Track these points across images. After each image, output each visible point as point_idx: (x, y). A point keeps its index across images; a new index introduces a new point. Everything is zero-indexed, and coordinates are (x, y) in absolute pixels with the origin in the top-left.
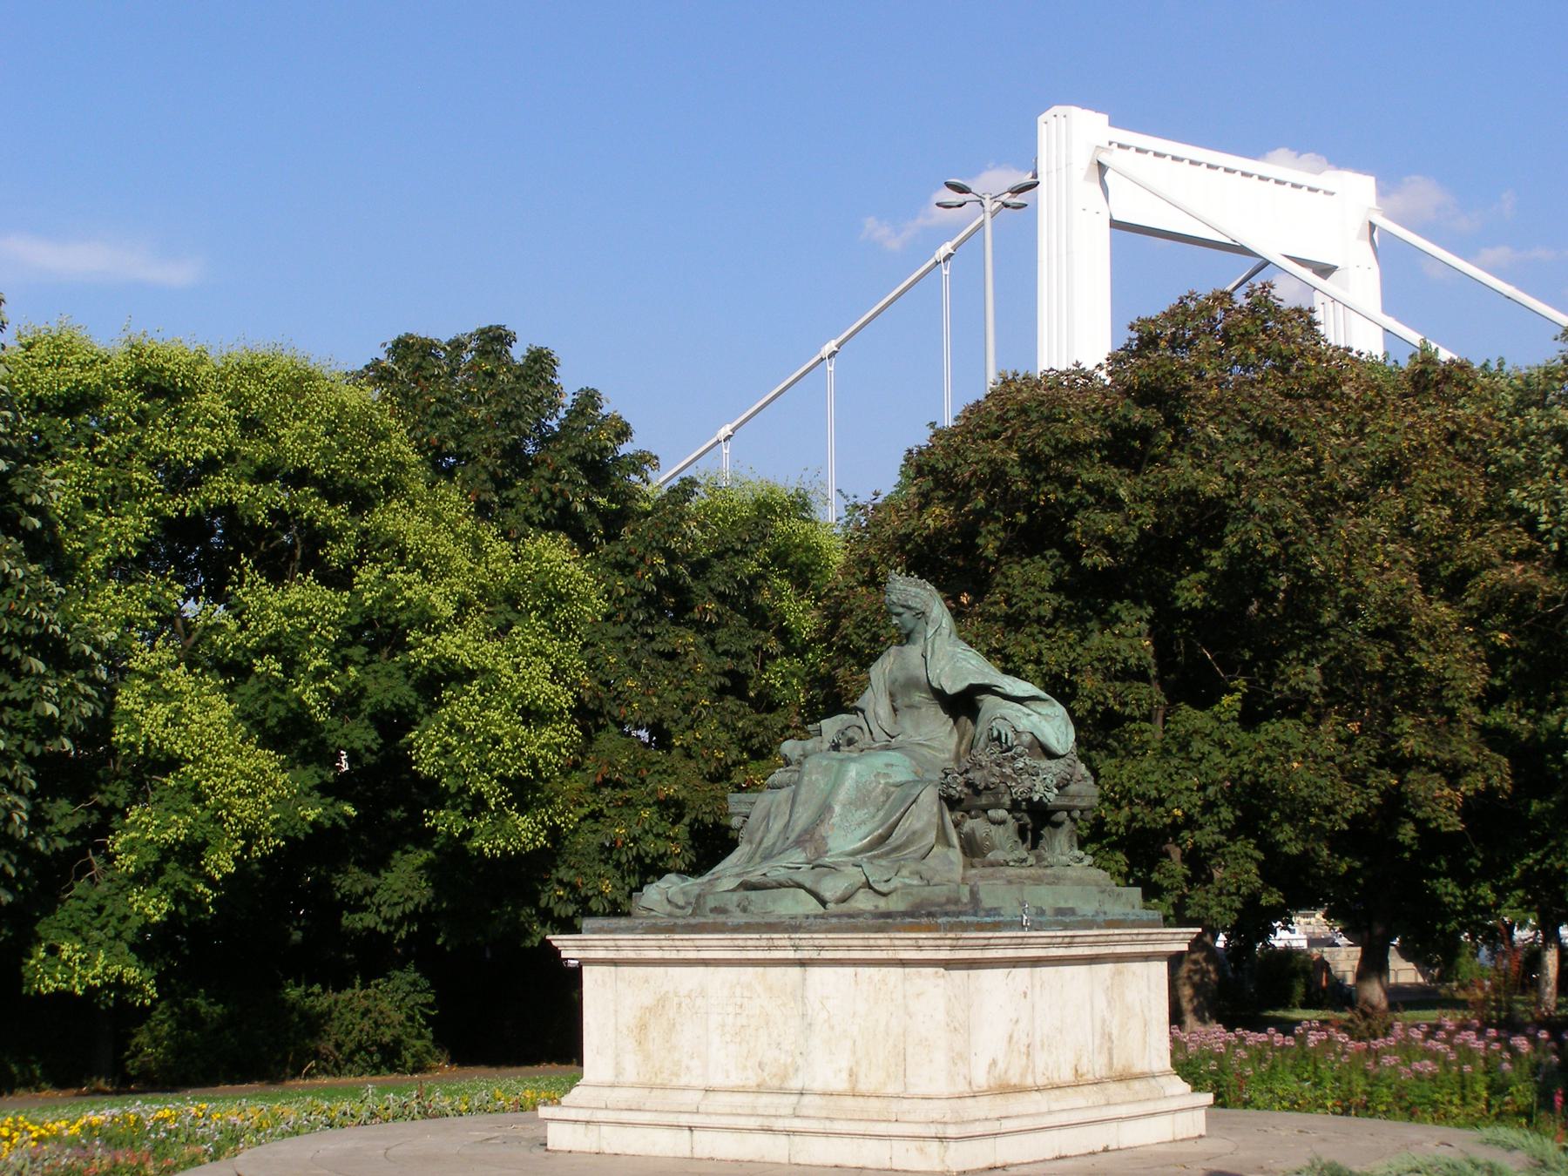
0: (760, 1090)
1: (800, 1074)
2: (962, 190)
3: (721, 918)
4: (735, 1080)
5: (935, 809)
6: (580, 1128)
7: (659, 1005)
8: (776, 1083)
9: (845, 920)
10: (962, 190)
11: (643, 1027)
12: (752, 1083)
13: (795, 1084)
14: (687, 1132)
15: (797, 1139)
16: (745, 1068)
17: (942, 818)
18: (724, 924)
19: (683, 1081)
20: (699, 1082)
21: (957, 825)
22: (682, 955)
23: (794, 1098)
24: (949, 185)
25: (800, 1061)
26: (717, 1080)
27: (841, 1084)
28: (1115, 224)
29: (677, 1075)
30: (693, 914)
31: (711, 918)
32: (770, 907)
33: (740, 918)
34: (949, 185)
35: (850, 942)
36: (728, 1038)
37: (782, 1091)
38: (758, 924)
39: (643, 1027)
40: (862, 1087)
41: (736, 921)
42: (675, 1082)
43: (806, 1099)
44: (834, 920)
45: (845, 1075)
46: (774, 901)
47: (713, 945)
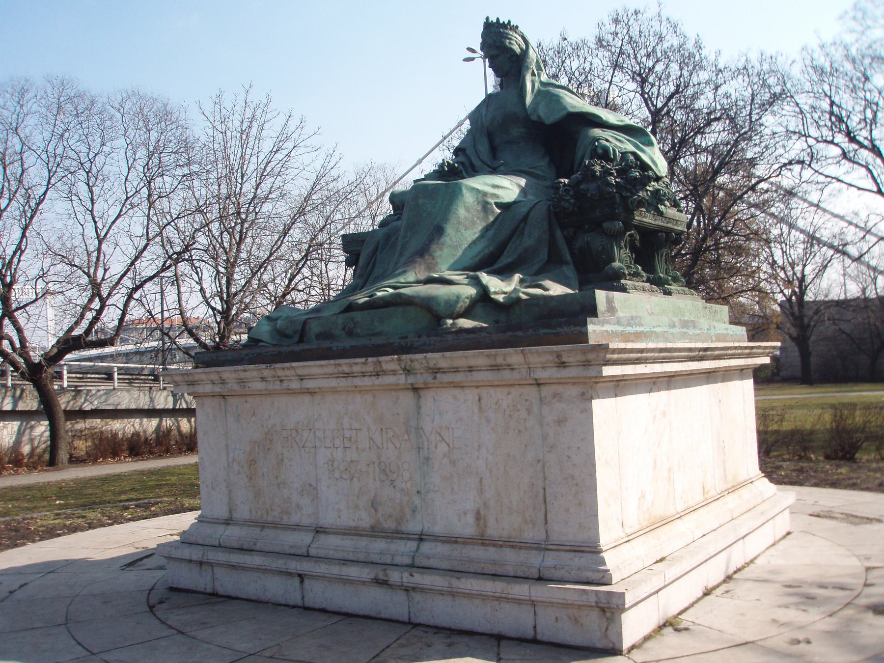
0: (375, 532)
1: (418, 517)
3: (326, 344)
4: (347, 520)
5: (546, 226)
11: (252, 462)
13: (414, 527)
14: (297, 580)
15: (417, 597)
17: (552, 235)
18: (329, 349)
21: (569, 241)
23: (412, 545)
24: (469, 49)
25: (417, 501)
26: (328, 519)
27: (467, 527)
30: (301, 341)
31: (314, 345)
33: (348, 343)
34: (469, 49)
36: (337, 475)
37: (398, 534)
39: (252, 462)
40: (493, 531)
41: (341, 345)
42: (286, 520)
45: (470, 519)
47: (317, 370)
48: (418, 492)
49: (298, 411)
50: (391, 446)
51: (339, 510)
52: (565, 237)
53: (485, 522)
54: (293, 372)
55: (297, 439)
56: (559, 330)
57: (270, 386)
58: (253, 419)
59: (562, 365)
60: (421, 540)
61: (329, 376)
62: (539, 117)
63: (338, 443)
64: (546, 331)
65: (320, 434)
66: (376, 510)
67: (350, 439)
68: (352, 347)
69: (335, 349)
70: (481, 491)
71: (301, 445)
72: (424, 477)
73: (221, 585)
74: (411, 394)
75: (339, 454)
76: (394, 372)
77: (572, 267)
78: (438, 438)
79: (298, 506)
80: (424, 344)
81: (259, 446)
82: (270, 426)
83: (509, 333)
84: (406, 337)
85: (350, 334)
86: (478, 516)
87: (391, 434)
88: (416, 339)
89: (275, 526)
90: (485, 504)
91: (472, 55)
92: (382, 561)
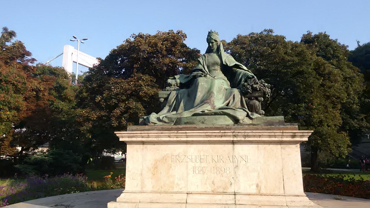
0: (214, 193)
1: (233, 186)
2: (75, 38)
7: (164, 159)
8: (221, 190)
9: (251, 126)
10: (75, 38)
11: (156, 167)
12: (209, 190)
13: (231, 190)
18: (196, 127)
19: (176, 190)
20: (185, 190)
22: (179, 139)
26: (191, 189)
27: (253, 190)
28: (74, 62)
32: (215, 122)
33: (203, 126)
35: (260, 134)
37: (224, 193)
38: (211, 127)
40: (263, 191)
42: (171, 190)
43: (238, 197)
44: (246, 126)
45: (254, 187)
46: (216, 119)
48: (233, 178)
51: (197, 185)
52: (245, 101)
53: (260, 188)
54: (185, 134)
55: (179, 159)
56: (287, 126)
57: (172, 139)
59: (294, 136)
60: (235, 194)
62: (227, 64)
63: (198, 160)
64: (282, 126)
66: (214, 185)
68: (205, 127)
70: (258, 177)
71: (181, 161)
72: (235, 173)
75: (198, 164)
76: (229, 136)
77: (247, 110)
79: (177, 184)
80: (236, 128)
83: (269, 126)
84: (229, 125)
85: (203, 123)
86: (257, 186)
88: (233, 126)
89: (166, 193)
90: (260, 181)
91: (74, 39)
92: (221, 203)
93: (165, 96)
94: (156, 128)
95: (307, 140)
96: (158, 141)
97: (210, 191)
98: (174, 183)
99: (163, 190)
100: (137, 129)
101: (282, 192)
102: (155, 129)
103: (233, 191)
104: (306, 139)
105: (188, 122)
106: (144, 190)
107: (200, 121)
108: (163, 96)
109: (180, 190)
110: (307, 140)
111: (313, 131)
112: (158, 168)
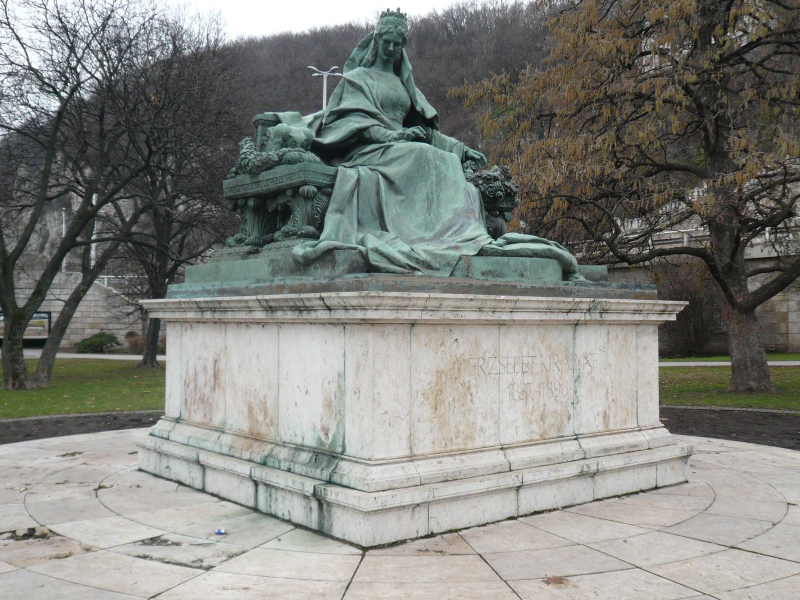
0: (544, 440)
1: (571, 421)
4: (523, 436)
6: (406, 515)
7: (459, 364)
8: (553, 433)
13: (569, 431)
16: (531, 422)
19: (478, 443)
26: (508, 438)
29: (473, 438)
36: (516, 397)
37: (561, 438)
42: (470, 445)
49: (488, 340)
50: (556, 369)
51: (517, 427)
55: (484, 367)
58: (442, 349)
61: (538, 310)
63: (518, 369)
65: (504, 362)
66: (544, 422)
67: (528, 365)
68: (532, 287)
69: (519, 287)
71: (487, 372)
72: (576, 392)
73: (438, 523)
74: (571, 328)
75: (518, 378)
78: (585, 361)
79: (481, 429)
81: (446, 376)
82: (458, 356)
86: (605, 416)
87: (556, 359)
89: (463, 452)
93: (321, 181)
94: (438, 283)
95: (675, 319)
96: (456, 320)
97: (538, 437)
98: (475, 428)
99: (454, 447)
100: (396, 284)
101: (632, 424)
102: (437, 286)
103: (571, 433)
104: (673, 318)
105: (490, 271)
106: (418, 451)
107: (516, 271)
108: (316, 180)
109: (488, 443)
110: (675, 319)
111: (687, 303)
112: (444, 391)
